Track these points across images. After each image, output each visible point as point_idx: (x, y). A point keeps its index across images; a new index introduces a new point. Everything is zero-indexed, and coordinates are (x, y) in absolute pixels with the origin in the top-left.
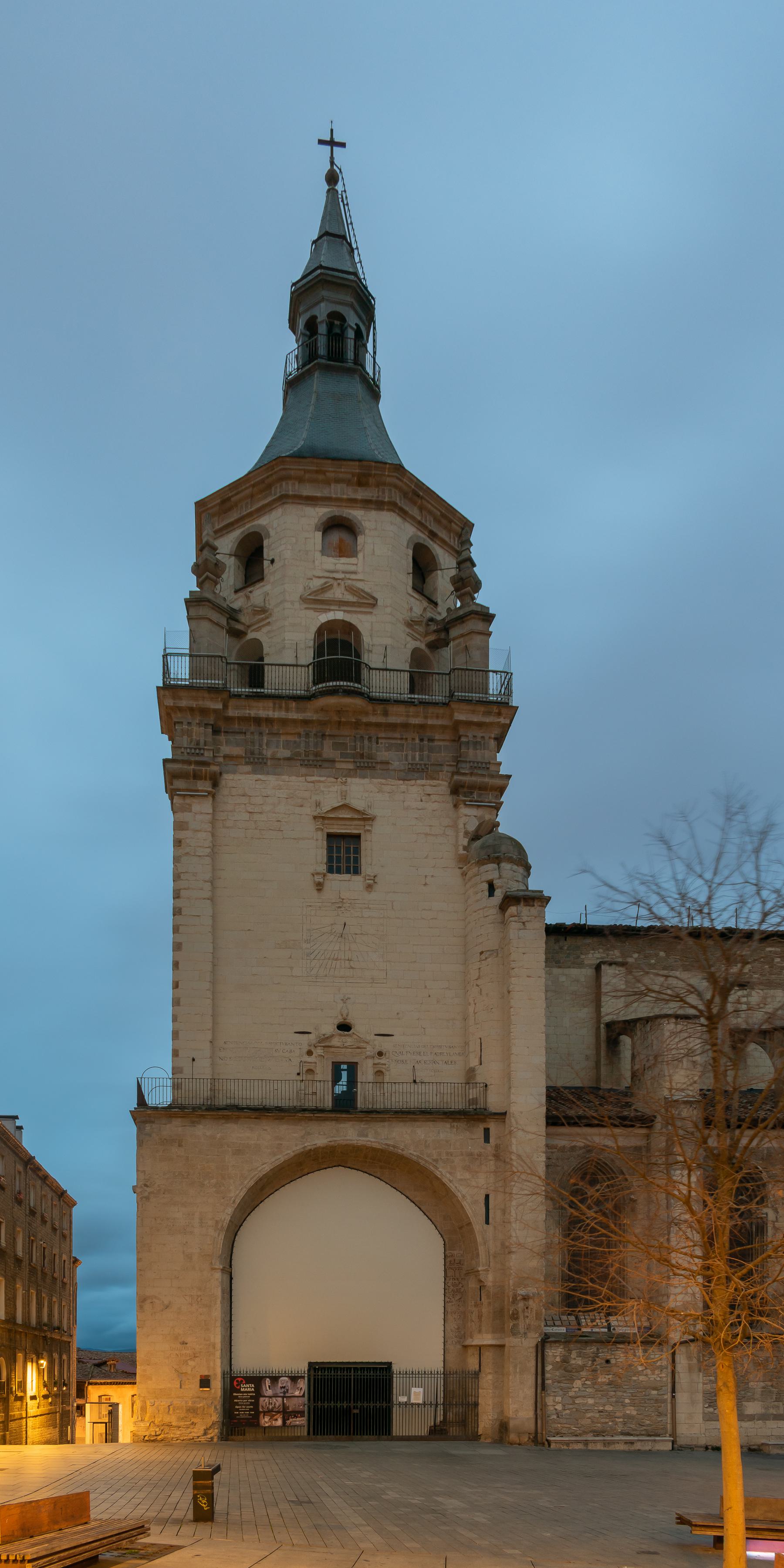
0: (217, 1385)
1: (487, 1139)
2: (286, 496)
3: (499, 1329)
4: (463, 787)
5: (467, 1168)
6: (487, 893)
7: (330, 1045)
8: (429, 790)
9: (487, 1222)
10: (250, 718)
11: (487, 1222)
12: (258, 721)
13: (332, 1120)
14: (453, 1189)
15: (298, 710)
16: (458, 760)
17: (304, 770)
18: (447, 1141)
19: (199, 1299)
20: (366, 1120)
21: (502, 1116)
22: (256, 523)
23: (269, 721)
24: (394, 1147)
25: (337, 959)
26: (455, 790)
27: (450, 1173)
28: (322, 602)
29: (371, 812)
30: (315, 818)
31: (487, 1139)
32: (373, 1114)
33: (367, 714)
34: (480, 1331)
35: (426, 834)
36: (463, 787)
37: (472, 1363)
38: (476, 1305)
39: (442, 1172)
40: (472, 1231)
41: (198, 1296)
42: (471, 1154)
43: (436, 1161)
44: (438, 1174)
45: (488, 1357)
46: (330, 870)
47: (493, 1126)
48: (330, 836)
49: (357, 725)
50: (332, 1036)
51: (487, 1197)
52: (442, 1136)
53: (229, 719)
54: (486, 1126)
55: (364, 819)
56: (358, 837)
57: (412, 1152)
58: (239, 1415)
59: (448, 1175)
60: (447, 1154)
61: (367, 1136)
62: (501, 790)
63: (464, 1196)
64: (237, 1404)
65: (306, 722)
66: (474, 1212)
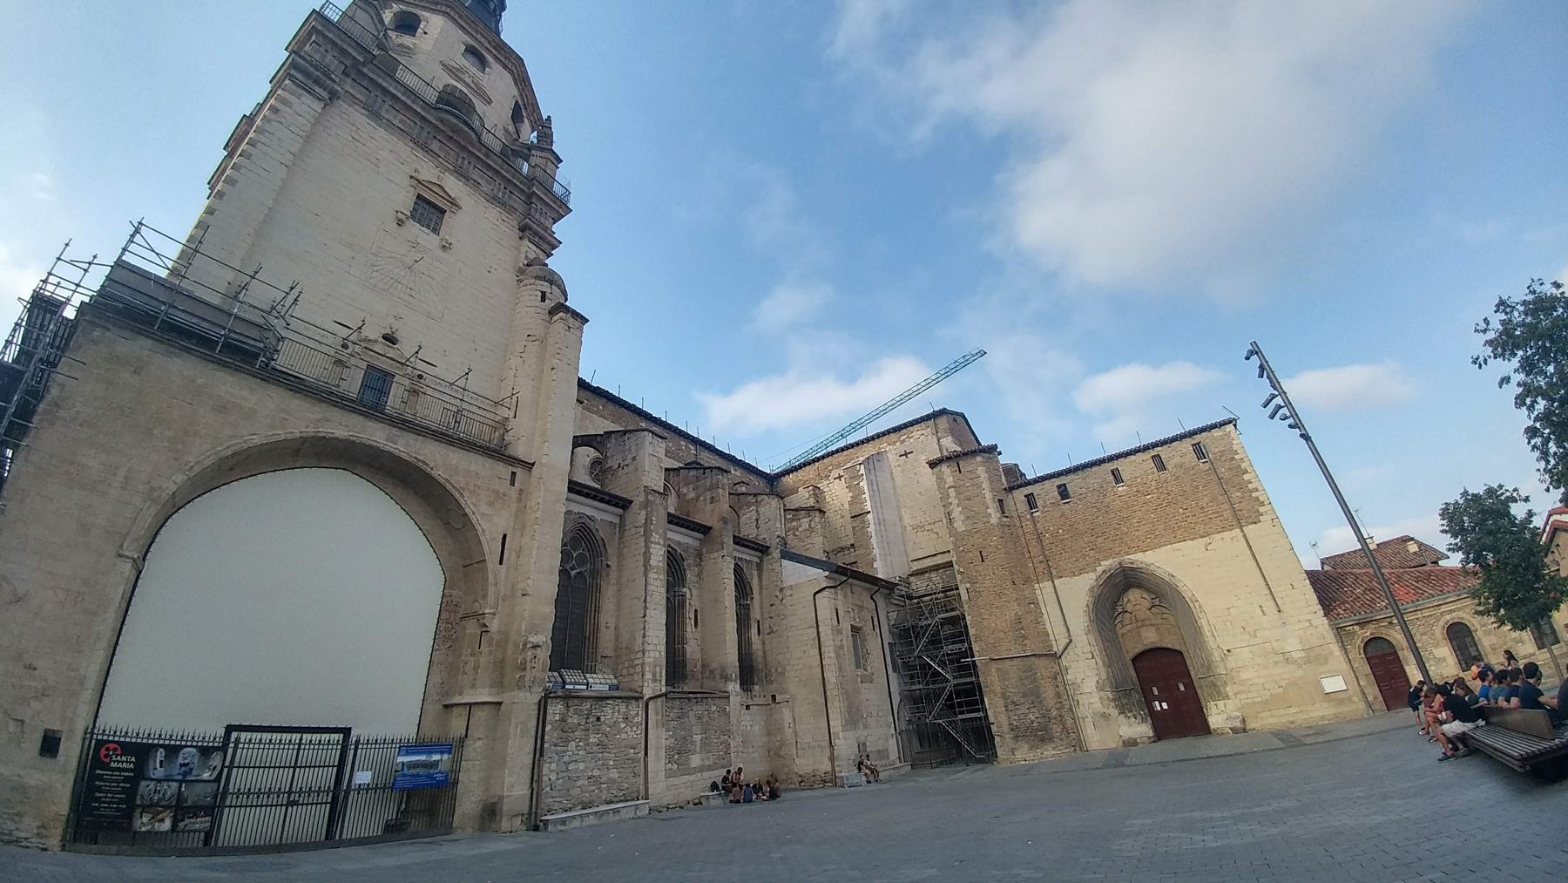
0: (71, 751)
1: (512, 483)
2: (449, 14)
3: (499, 684)
4: (530, 229)
5: (491, 504)
6: (540, 299)
7: (371, 348)
8: (504, 218)
9: (501, 563)
10: (381, 86)
11: (501, 563)
12: (385, 91)
13: (360, 414)
14: (474, 521)
15: (422, 108)
16: (528, 215)
17: (412, 144)
18: (477, 474)
19: (80, 598)
20: (400, 428)
21: (529, 466)
22: (423, 13)
23: (394, 97)
24: (424, 462)
25: (399, 283)
26: (523, 229)
27: (474, 505)
28: (457, 76)
29: (461, 203)
30: (411, 177)
31: (512, 483)
32: (402, 424)
33: (474, 147)
34: (473, 686)
35: (497, 241)
36: (530, 229)
37: (457, 726)
38: (473, 654)
39: (468, 503)
40: (484, 570)
41: (79, 593)
42: (497, 492)
43: (464, 489)
44: (462, 502)
45: (480, 715)
46: (413, 217)
47: (519, 471)
48: (419, 197)
49: (464, 148)
50: (376, 341)
51: (505, 536)
52: (473, 467)
53: (361, 73)
54: (514, 471)
55: (452, 203)
56: (443, 212)
57: (439, 473)
58: (98, 808)
59: (472, 507)
60: (475, 486)
61: (396, 444)
62: (554, 247)
63: (483, 531)
64: (99, 789)
65: (424, 119)
66: (491, 549)
